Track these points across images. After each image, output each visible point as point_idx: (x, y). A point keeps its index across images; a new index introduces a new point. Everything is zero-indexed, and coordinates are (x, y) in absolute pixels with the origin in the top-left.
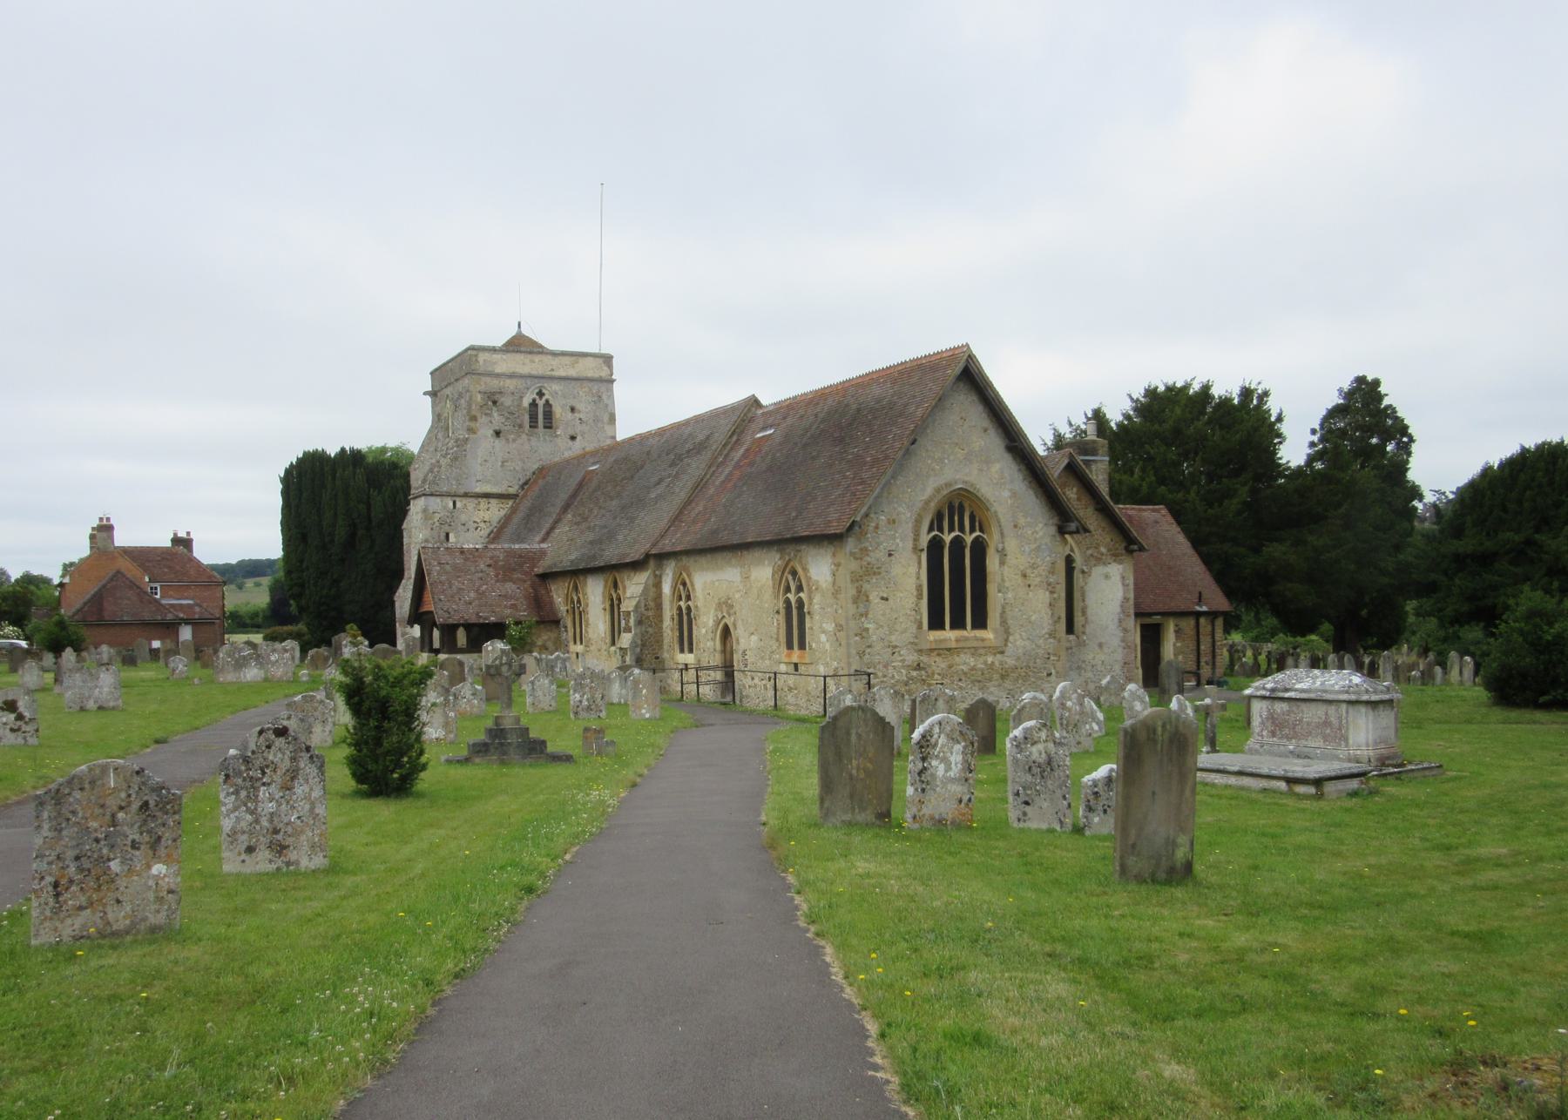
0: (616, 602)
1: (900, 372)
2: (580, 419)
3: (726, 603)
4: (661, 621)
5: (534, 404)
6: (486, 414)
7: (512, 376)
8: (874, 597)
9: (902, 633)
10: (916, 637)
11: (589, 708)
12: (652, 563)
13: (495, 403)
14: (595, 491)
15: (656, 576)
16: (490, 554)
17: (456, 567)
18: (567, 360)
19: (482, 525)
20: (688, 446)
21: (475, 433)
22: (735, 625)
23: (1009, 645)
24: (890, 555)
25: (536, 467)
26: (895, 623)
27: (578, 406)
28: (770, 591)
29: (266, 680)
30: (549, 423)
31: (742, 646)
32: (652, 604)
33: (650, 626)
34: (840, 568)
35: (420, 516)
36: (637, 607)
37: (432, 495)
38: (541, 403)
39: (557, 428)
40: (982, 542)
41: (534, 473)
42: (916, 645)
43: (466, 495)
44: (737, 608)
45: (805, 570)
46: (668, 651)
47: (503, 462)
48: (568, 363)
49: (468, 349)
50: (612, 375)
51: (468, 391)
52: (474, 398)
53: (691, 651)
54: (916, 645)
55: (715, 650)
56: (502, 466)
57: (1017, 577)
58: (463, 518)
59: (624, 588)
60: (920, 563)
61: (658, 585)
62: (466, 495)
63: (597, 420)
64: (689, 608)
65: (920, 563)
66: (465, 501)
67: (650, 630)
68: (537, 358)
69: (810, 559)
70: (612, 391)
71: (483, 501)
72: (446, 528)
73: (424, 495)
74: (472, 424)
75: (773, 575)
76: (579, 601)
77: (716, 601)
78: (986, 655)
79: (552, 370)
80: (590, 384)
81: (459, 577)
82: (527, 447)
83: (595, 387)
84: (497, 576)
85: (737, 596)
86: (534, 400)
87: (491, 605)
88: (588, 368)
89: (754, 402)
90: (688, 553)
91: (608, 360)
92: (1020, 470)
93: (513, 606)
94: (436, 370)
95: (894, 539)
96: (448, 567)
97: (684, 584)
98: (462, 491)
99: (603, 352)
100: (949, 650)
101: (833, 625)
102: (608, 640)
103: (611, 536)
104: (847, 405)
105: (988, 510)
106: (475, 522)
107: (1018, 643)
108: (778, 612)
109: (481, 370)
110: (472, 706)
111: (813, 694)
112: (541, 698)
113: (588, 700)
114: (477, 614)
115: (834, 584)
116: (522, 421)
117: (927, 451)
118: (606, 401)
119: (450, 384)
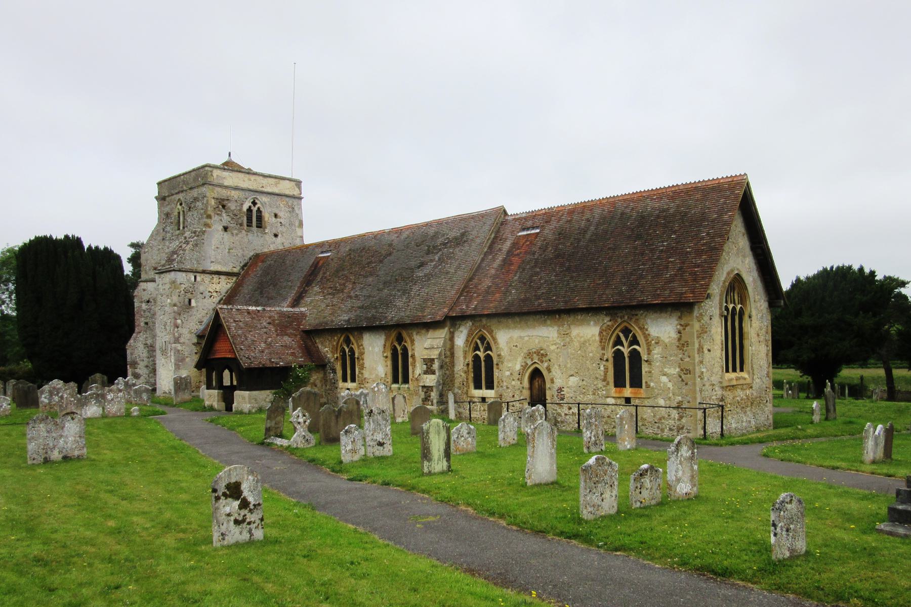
0: (400, 351)
1: (674, 192)
2: (281, 223)
3: (538, 353)
4: (453, 366)
5: (249, 210)
6: (218, 214)
7: (236, 188)
8: (706, 351)
11: (595, 444)
12: (448, 323)
13: (224, 206)
14: (337, 271)
15: (450, 332)
16: (267, 315)
17: (246, 324)
19: (215, 294)
20: (440, 240)
21: (210, 227)
22: (549, 370)
24: (711, 319)
25: (252, 254)
26: (713, 368)
27: (280, 214)
28: (597, 344)
29: (104, 416)
30: (260, 225)
31: (558, 383)
32: (448, 353)
33: (448, 369)
34: (688, 329)
35: (168, 286)
36: (440, 355)
37: (180, 271)
38: (255, 209)
39: (266, 228)
41: (250, 259)
43: (204, 272)
44: (552, 356)
45: (642, 329)
46: (459, 388)
47: (229, 250)
49: (203, 167)
50: (301, 194)
51: (205, 196)
52: (209, 202)
53: (490, 386)
55: (523, 388)
56: (229, 252)
58: (202, 288)
59: (412, 341)
60: (722, 325)
61: (452, 339)
62: (204, 272)
63: (291, 224)
64: (489, 359)
65: (722, 325)
66: (203, 276)
67: (447, 372)
68: (253, 177)
69: (649, 321)
70: (301, 205)
71: (216, 277)
72: (189, 295)
73: (174, 270)
74: (208, 221)
75: (601, 333)
76: (352, 351)
77: (525, 351)
79: (263, 187)
80: (287, 199)
81: (250, 331)
82: (246, 240)
83: (290, 201)
84: (276, 331)
85: (553, 347)
86: (250, 207)
87: (277, 353)
88: (286, 188)
89: (505, 211)
90: (489, 316)
91: (298, 183)
92: (755, 263)
93: (293, 354)
94: (165, 181)
96: (241, 324)
97: (483, 339)
98: (201, 269)
99: (294, 177)
100: (733, 386)
101: (678, 370)
102: (390, 379)
103: (387, 303)
104: (622, 214)
106: (209, 292)
108: (607, 360)
109: (215, 182)
110: (468, 444)
111: (650, 420)
112: (509, 433)
113: (594, 436)
114: (270, 360)
115: (679, 339)
116: (243, 221)
118: (297, 212)
119: (182, 191)
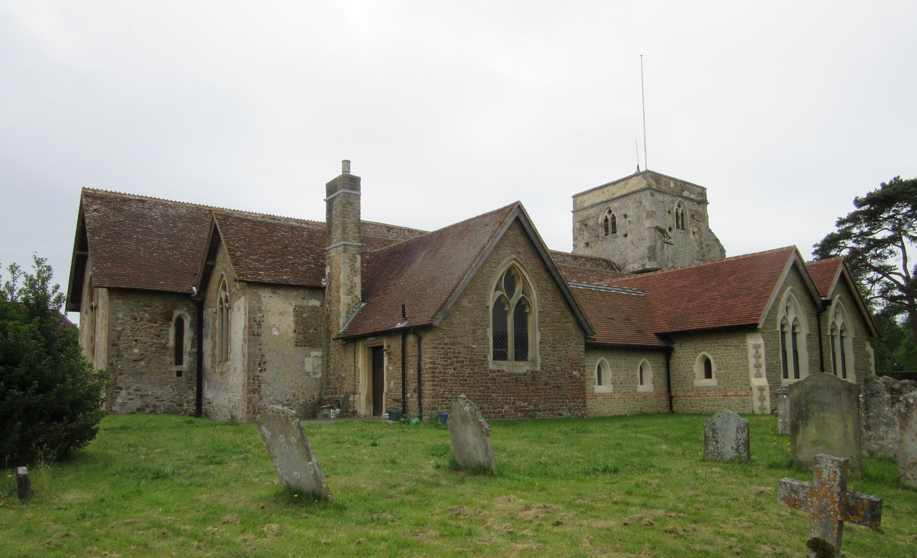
2: (629, 222)
18: (619, 185)
27: (629, 213)
48: (622, 186)
68: (605, 190)
79: (614, 194)
80: (634, 196)
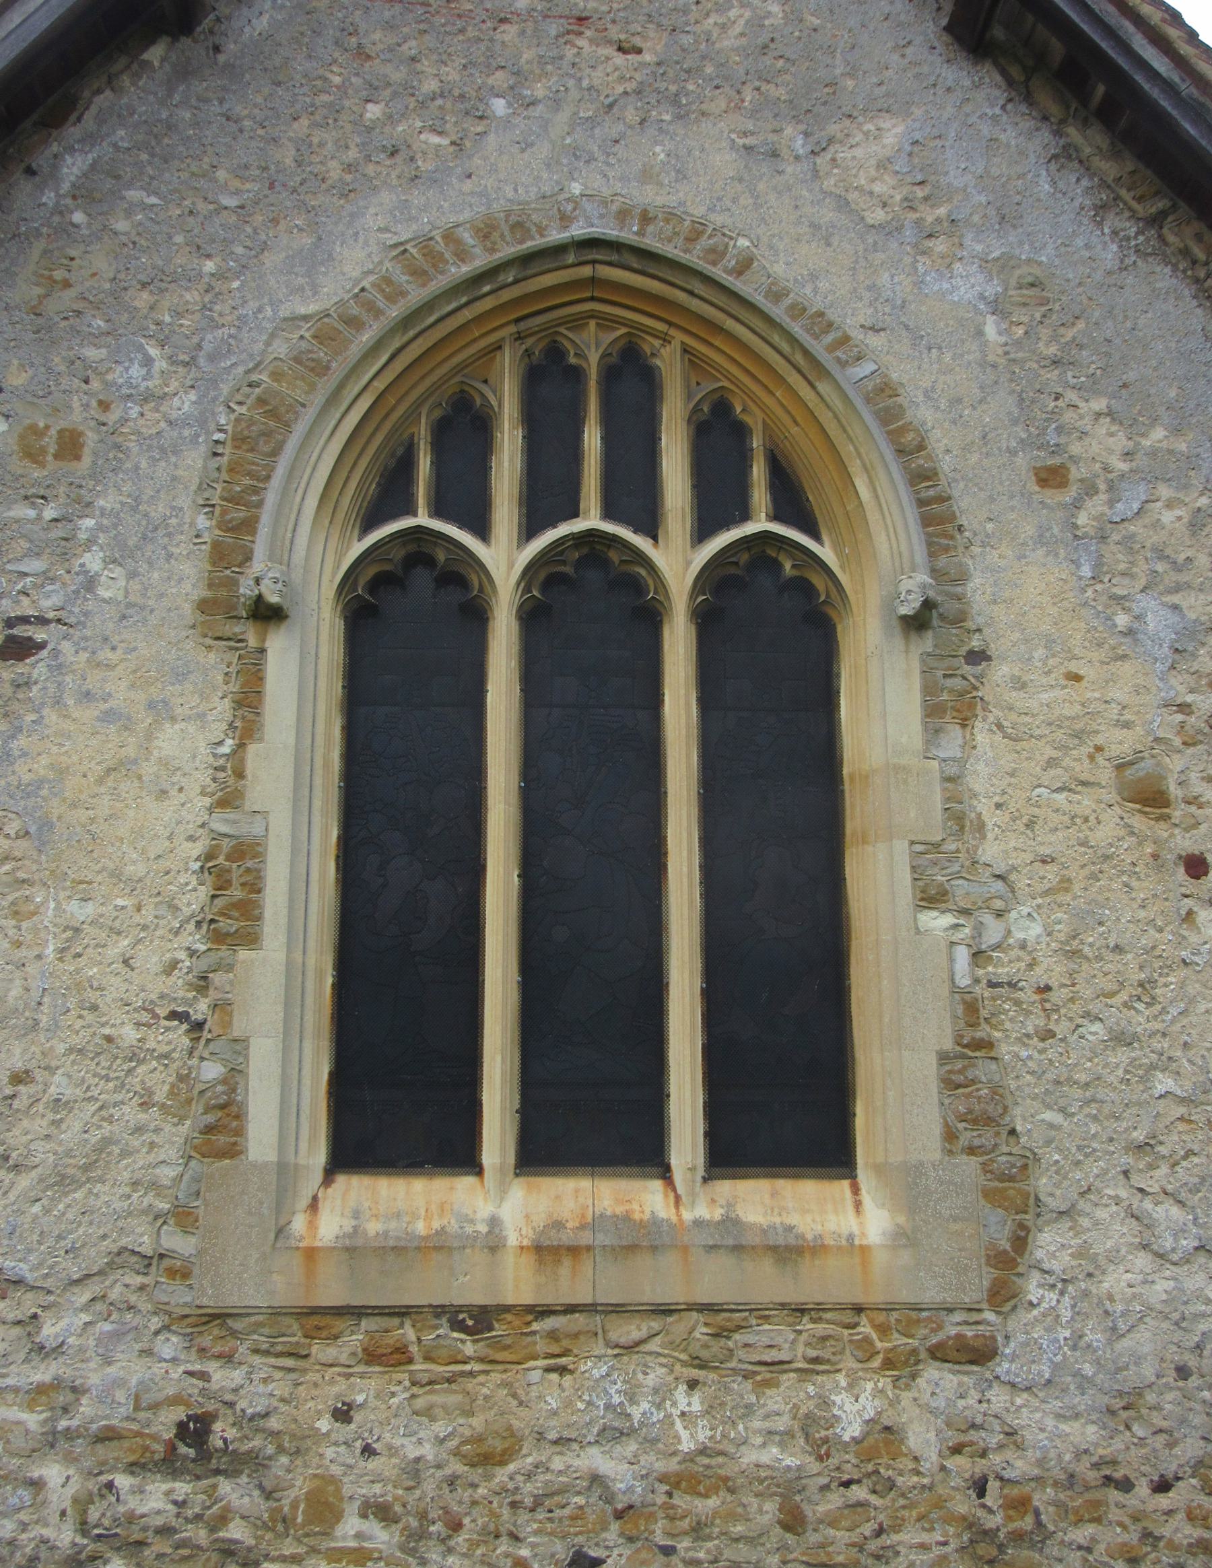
9: (63, 1182)
10: (184, 1217)
23: (1033, 1289)
40: (803, 587)
42: (181, 1273)
54: (181, 1273)
57: (1086, 802)
78: (815, 1366)
92: (1065, 155)
95: (67, 548)
105: (814, 369)
107: (1115, 1281)
117: (362, 54)
